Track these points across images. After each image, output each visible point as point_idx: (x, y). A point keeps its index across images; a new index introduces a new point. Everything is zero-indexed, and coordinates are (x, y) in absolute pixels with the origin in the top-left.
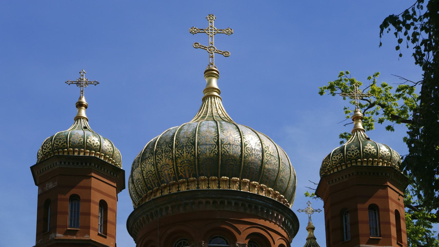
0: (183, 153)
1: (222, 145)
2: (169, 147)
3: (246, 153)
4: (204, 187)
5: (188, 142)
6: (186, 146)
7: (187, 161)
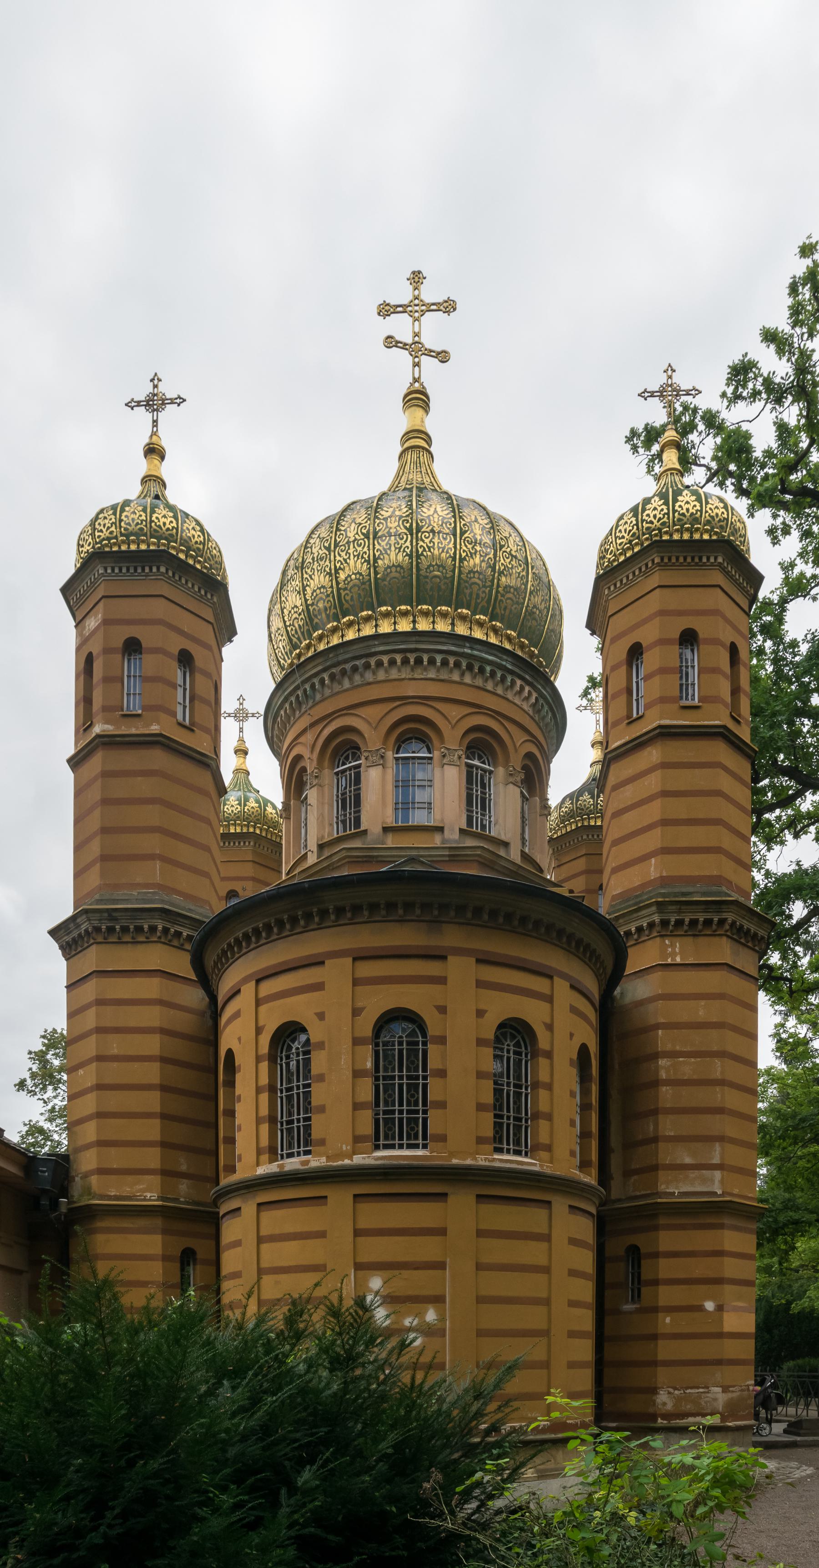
0: (349, 558)
1: (420, 535)
2: (325, 547)
3: (464, 551)
4: (386, 627)
5: (357, 533)
6: (354, 541)
7: (355, 574)
